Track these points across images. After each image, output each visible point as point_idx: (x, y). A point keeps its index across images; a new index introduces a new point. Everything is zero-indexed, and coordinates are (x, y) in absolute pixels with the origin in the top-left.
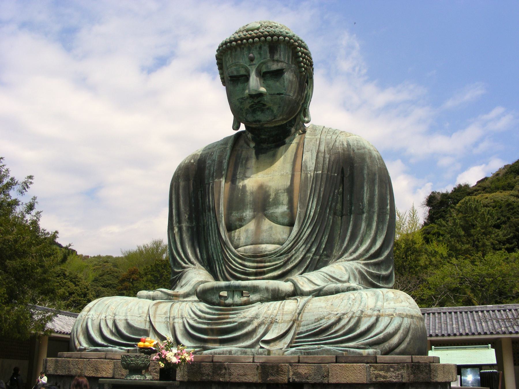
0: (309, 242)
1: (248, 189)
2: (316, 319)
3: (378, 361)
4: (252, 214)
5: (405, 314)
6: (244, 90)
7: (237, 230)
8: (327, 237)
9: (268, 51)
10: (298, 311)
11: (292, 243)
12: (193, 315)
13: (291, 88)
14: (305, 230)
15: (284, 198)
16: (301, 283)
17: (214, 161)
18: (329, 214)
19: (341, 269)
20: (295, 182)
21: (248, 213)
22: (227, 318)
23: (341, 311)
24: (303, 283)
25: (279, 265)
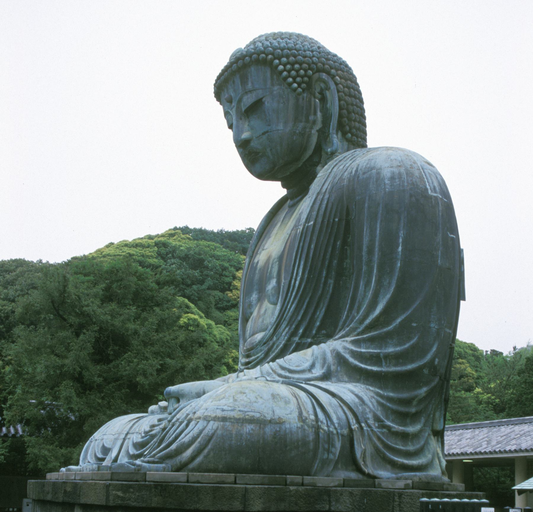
0: (294, 322)
3: (148, 479)
5: (214, 415)
8: (324, 310)
9: (240, 83)
14: (289, 307)
18: (327, 277)
21: (254, 296)
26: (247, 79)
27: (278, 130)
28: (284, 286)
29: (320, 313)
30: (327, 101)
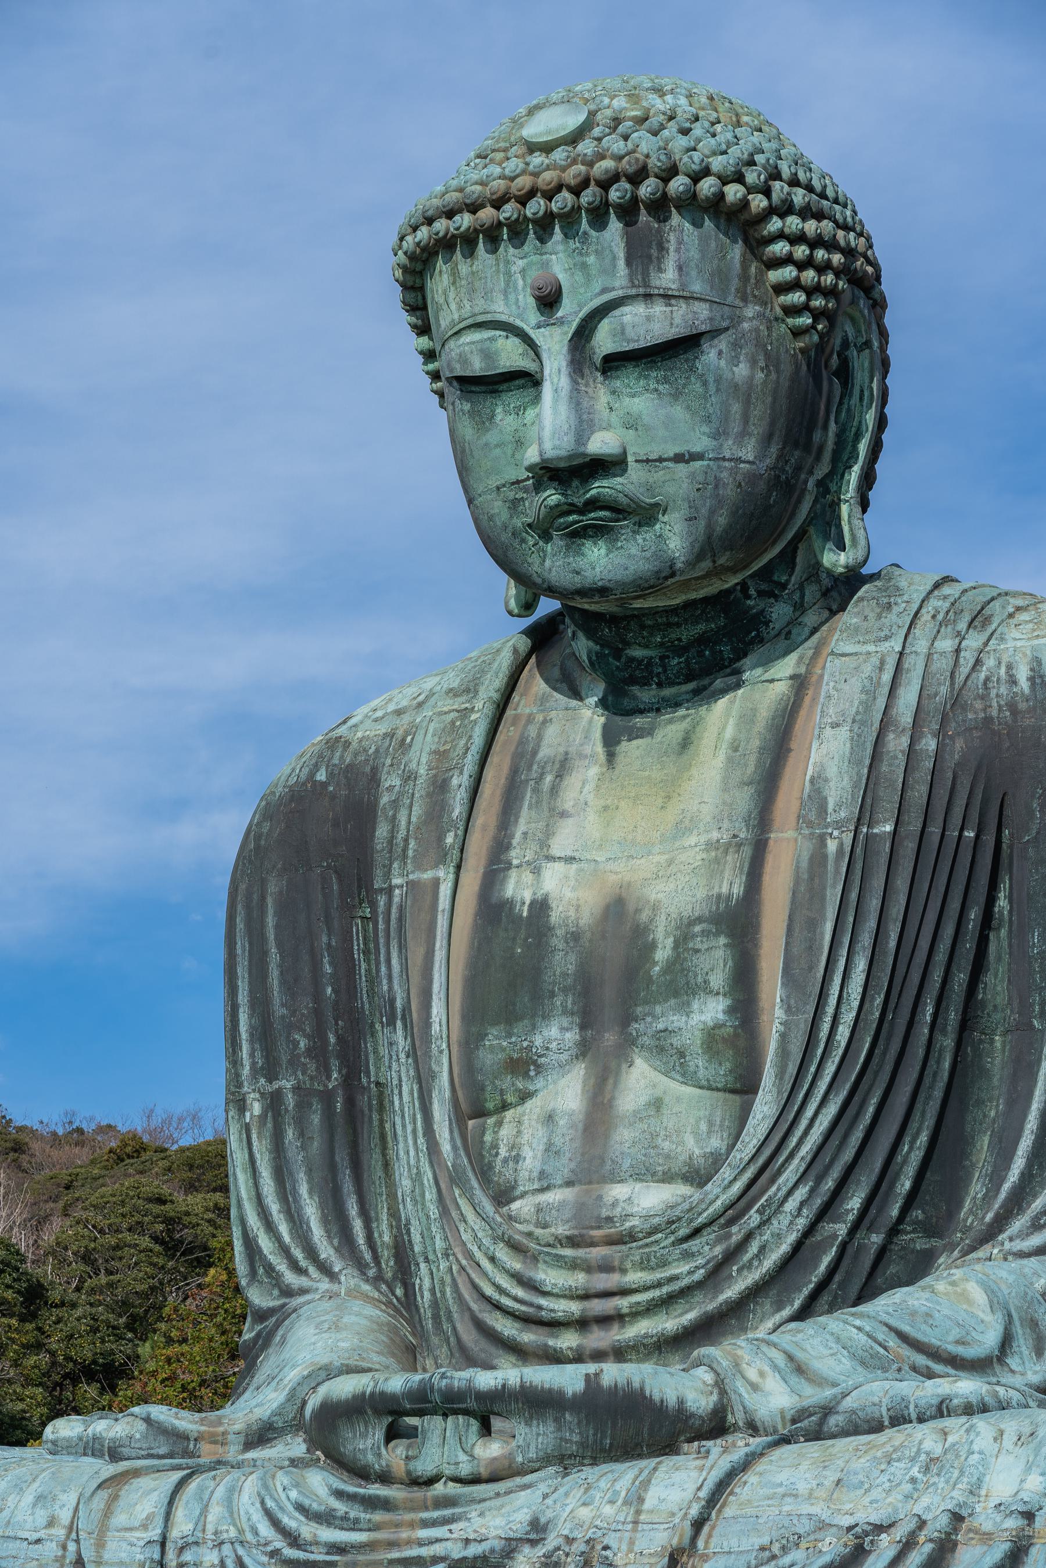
1: (555, 917)
2: (763, 1549)
4: (572, 1036)
6: (520, 443)
7: (509, 1114)
9: (621, 255)
10: (694, 1511)
11: (749, 1174)
12: (266, 1530)
13: (746, 419)
14: (809, 1112)
15: (715, 962)
16: (752, 1374)
17: (409, 777)
19: (970, 1302)
20: (766, 879)
21: (556, 1034)
22: (409, 1542)
23: (867, 1514)
24: (762, 1374)
25: (686, 1282)
26: (662, 248)
27: (739, 460)
28: (784, 1037)
29: (911, 1149)
30: (853, 385)
